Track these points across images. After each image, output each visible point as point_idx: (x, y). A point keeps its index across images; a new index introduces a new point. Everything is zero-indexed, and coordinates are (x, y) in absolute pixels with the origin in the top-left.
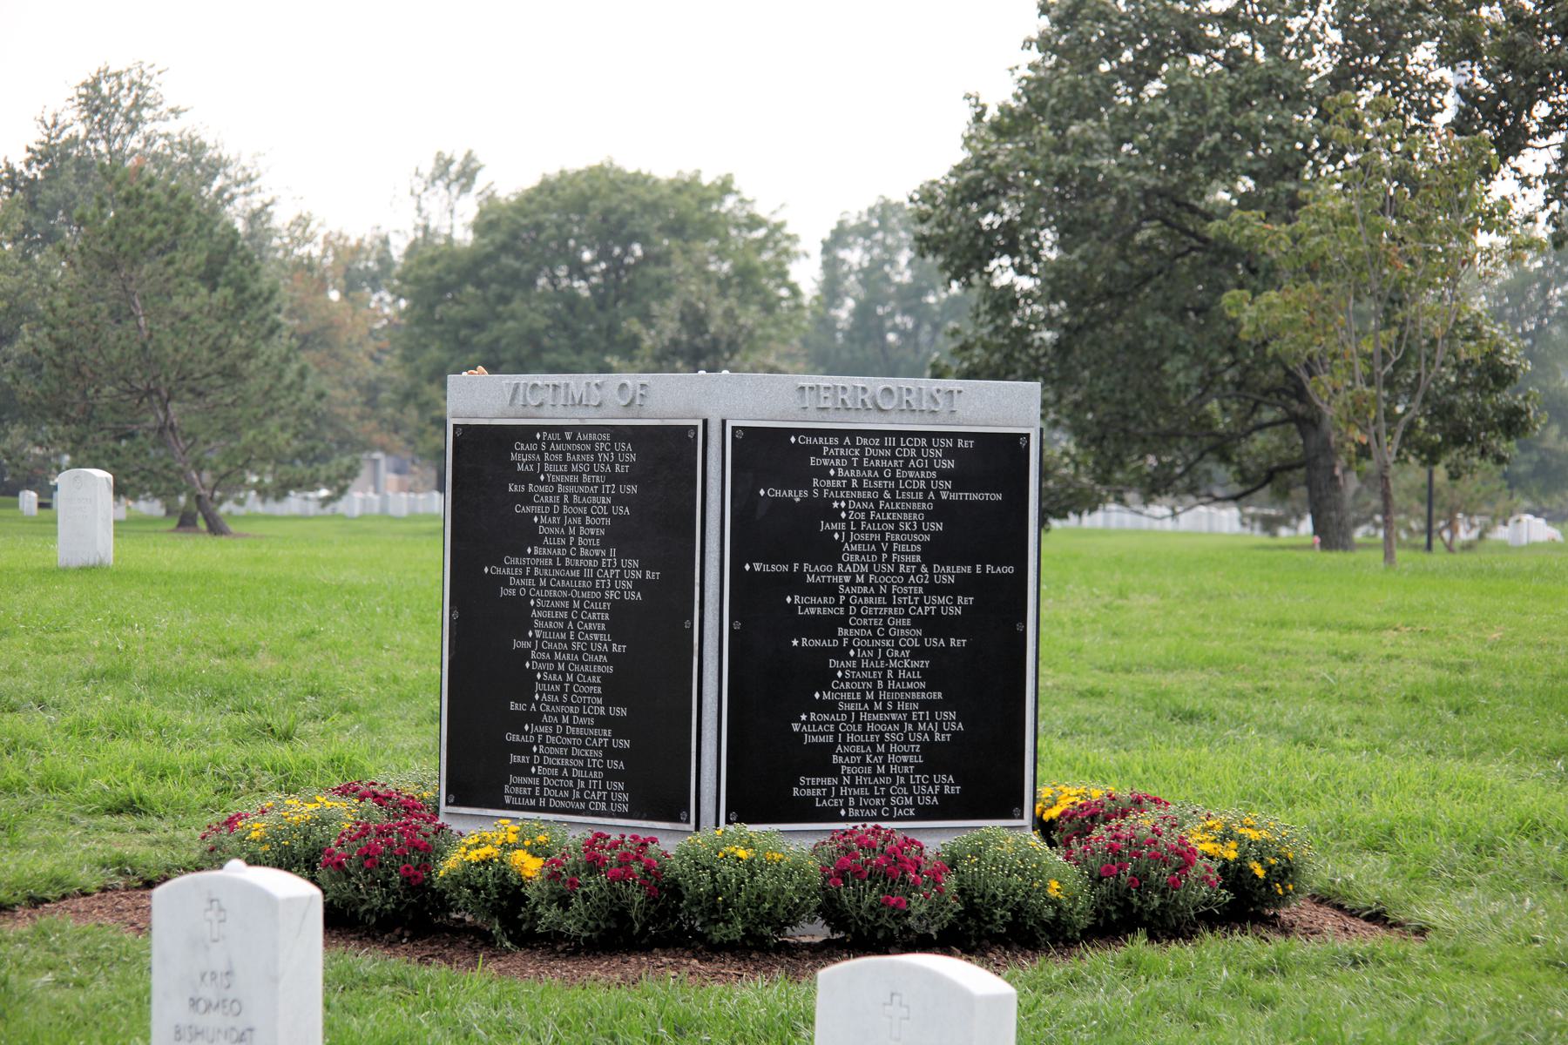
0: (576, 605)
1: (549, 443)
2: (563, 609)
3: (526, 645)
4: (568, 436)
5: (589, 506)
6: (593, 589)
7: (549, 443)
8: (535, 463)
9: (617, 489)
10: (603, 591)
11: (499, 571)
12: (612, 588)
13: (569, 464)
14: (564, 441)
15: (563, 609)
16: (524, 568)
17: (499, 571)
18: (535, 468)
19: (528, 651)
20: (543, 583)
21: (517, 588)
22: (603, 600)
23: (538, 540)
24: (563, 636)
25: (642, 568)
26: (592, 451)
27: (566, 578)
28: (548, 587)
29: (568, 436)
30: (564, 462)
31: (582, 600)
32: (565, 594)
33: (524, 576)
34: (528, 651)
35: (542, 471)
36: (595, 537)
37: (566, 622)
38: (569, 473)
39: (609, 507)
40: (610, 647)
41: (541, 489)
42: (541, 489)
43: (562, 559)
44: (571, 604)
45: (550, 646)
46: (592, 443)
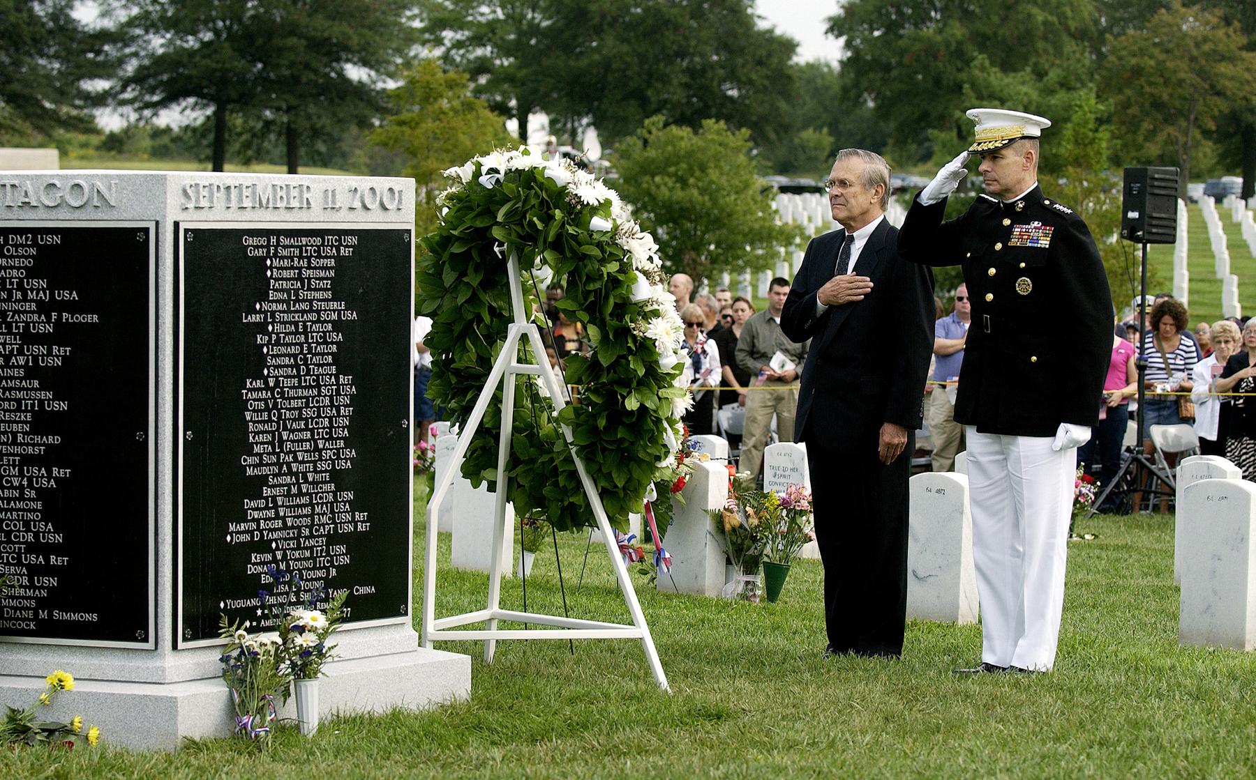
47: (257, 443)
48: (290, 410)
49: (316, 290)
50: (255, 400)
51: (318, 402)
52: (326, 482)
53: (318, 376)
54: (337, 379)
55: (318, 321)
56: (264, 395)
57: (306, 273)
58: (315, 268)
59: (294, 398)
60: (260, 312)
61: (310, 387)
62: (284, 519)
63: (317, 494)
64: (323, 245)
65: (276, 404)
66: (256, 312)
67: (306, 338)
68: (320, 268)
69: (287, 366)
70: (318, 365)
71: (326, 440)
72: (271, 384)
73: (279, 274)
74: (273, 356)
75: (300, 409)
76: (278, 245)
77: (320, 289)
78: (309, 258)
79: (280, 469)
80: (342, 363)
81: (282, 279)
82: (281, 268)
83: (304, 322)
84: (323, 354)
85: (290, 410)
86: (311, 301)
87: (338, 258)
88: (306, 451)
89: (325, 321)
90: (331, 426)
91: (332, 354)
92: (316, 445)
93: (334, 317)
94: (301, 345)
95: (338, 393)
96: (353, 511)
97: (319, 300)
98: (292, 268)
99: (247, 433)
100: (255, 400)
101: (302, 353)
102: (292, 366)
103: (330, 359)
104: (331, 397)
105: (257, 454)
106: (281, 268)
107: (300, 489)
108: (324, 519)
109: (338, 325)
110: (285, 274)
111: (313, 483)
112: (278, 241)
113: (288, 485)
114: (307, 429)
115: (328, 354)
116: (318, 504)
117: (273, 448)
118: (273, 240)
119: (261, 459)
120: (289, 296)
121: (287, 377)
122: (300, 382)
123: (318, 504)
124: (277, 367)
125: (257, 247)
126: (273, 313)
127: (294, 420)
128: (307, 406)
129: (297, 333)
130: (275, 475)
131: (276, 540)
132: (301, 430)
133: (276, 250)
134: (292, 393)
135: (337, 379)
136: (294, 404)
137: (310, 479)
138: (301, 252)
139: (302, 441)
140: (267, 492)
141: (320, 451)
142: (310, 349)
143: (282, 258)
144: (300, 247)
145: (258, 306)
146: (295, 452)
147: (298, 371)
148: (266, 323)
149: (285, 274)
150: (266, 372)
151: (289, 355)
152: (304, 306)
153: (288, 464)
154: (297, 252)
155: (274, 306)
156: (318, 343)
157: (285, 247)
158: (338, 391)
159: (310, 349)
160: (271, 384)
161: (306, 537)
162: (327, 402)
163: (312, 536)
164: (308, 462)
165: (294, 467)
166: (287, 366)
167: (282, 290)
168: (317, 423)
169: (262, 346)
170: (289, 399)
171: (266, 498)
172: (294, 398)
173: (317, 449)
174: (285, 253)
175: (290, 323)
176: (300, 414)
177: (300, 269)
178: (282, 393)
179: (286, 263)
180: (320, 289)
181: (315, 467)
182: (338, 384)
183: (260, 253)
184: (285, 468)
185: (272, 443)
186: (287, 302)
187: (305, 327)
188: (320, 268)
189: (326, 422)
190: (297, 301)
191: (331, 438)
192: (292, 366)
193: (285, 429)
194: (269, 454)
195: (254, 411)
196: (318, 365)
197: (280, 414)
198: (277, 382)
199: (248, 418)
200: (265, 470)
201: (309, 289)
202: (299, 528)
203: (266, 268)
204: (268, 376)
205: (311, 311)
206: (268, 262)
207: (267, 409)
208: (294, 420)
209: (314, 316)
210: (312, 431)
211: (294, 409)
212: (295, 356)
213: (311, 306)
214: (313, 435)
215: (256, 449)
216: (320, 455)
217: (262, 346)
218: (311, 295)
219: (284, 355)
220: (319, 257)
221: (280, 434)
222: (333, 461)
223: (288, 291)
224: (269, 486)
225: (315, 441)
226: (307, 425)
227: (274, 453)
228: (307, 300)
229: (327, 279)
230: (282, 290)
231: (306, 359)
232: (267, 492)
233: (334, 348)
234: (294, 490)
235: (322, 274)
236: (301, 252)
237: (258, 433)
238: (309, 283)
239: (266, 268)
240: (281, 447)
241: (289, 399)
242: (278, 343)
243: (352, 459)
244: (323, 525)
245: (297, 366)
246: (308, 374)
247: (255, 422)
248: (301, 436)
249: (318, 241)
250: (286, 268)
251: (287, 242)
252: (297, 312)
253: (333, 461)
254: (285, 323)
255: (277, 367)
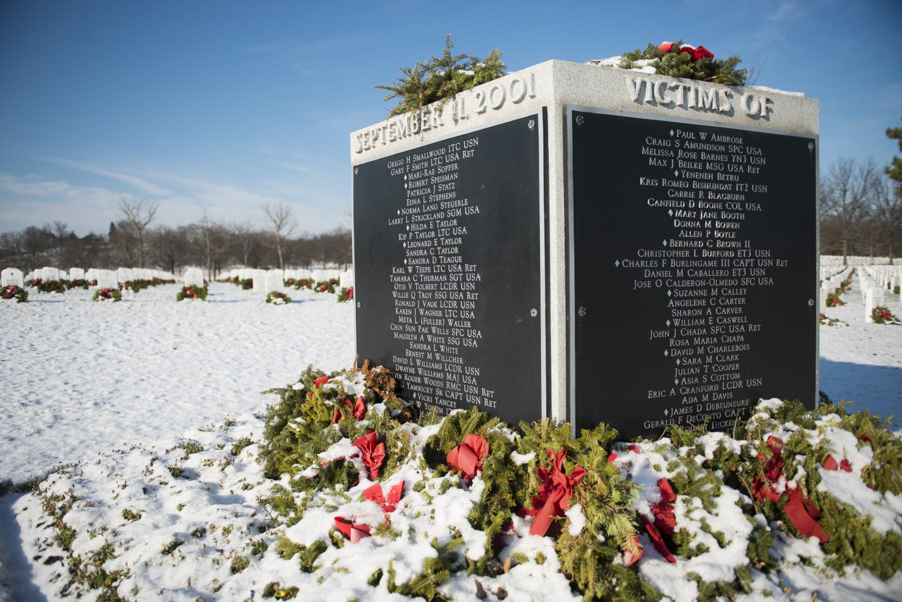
0: (714, 292)
1: (683, 141)
2: (700, 298)
3: (661, 334)
4: (703, 136)
5: (724, 202)
6: (730, 277)
7: (683, 141)
8: (669, 159)
9: (750, 188)
10: (739, 278)
11: (632, 264)
12: (748, 275)
13: (704, 163)
14: (698, 140)
15: (700, 298)
16: (659, 260)
17: (632, 264)
18: (669, 163)
19: (667, 340)
20: (680, 274)
21: (653, 279)
22: (739, 286)
23: (674, 234)
24: (703, 322)
25: (773, 257)
26: (726, 153)
27: (704, 269)
28: (686, 277)
29: (703, 136)
30: (699, 160)
31: (720, 288)
32: (702, 283)
33: (660, 268)
34: (667, 340)
35: (676, 167)
36: (730, 230)
37: (704, 309)
38: (704, 170)
39: (743, 204)
40: (746, 327)
41: (674, 184)
42: (674, 184)
43: (699, 251)
44: (709, 292)
45: (689, 333)
46: (726, 145)
47: (401, 315)
48: (425, 291)
49: (442, 192)
50: (399, 283)
51: (447, 286)
52: (455, 355)
53: (446, 265)
54: (463, 268)
55: (446, 218)
56: (404, 279)
57: (434, 180)
58: (441, 174)
59: (428, 283)
60: (400, 216)
61: (440, 274)
62: (422, 377)
63: (448, 363)
64: (447, 153)
65: (414, 286)
66: (398, 217)
67: (436, 234)
68: (445, 174)
69: (421, 257)
70: (447, 256)
71: (455, 319)
72: (410, 271)
73: (413, 185)
74: (411, 249)
75: (433, 292)
76: (412, 162)
77: (447, 191)
78: (436, 167)
79: (419, 337)
80: (467, 253)
81: (416, 188)
82: (416, 180)
83: (434, 220)
84: (450, 246)
85: (425, 291)
86: (439, 203)
87: (460, 162)
88: (438, 327)
89: (451, 218)
90: (459, 309)
91: (458, 245)
92: (447, 323)
93: (459, 213)
94: (432, 239)
95: (464, 280)
96: (480, 385)
97: (445, 201)
98: (423, 178)
99: (394, 307)
100: (399, 283)
101: (433, 245)
102: (426, 257)
103: (456, 250)
104: (458, 283)
105: (401, 324)
106: (416, 180)
107: (434, 356)
108: (454, 386)
109: (462, 221)
110: (418, 184)
111: (445, 354)
112: (412, 159)
113: (425, 352)
114: (438, 309)
115: (454, 246)
116: (449, 372)
117: (413, 321)
118: (408, 159)
119: (404, 328)
120: (422, 201)
121: (422, 265)
122: (432, 270)
123: (449, 372)
124: (415, 257)
125: (397, 168)
126: (410, 216)
127: (429, 300)
128: (438, 290)
129: (428, 230)
130: (415, 342)
131: (416, 392)
132: (434, 309)
133: (411, 167)
134: (426, 278)
135: (463, 268)
136: (427, 287)
137: (443, 350)
138: (429, 164)
139: (435, 318)
140: (408, 353)
141: (450, 328)
142: (439, 242)
143: (416, 172)
144: (429, 160)
145: (399, 212)
146: (430, 326)
147: (431, 261)
148: (405, 225)
149: (418, 184)
150: (405, 262)
151: (423, 249)
152: (433, 208)
153: (425, 335)
154: (426, 164)
155: (410, 211)
156: (446, 237)
157: (417, 163)
158: (464, 277)
159: (439, 242)
160: (410, 271)
161: (440, 397)
162: (455, 286)
163: (444, 398)
164: (440, 336)
165: (429, 337)
166: (421, 257)
167: (417, 197)
168: (447, 304)
169: (402, 242)
170: (425, 283)
171: (408, 358)
172: (428, 283)
173: (447, 326)
174: (417, 167)
175: (423, 222)
176: (433, 296)
177: (429, 177)
178: (419, 278)
179: (418, 175)
180: (447, 191)
181: (446, 341)
182: (464, 272)
183: (399, 172)
184: (422, 337)
185: (412, 316)
186: (420, 206)
187: (435, 224)
188: (445, 174)
189: (455, 304)
190: (428, 204)
191: (459, 319)
192: (426, 257)
193: (422, 306)
194: (410, 324)
195: (398, 291)
196: (447, 256)
197: (417, 295)
198: (414, 270)
199: (395, 296)
200: (407, 337)
201: (437, 193)
202: (434, 388)
203: (404, 182)
204: (407, 265)
205: (439, 211)
206: (405, 178)
207: (407, 290)
208: (429, 300)
209: (441, 215)
210: (443, 310)
211: (428, 291)
212: (428, 249)
213: (439, 206)
214: (443, 314)
215: (401, 320)
216: (450, 332)
217: (402, 242)
218: (439, 197)
219: (419, 248)
220: (445, 164)
221: (418, 312)
222: (461, 338)
223: (420, 197)
224: (410, 350)
225: (446, 319)
226: (438, 304)
227: (413, 324)
228: (436, 202)
229: (451, 181)
230: (417, 197)
231: (436, 251)
232: (408, 353)
233: (460, 241)
234: (430, 356)
235: (447, 178)
236: (429, 164)
237: (402, 307)
238: (437, 188)
239: (404, 182)
240: (418, 320)
241: (425, 283)
242: (414, 239)
243: (478, 340)
244: (454, 391)
245: (430, 257)
246: (438, 262)
247: (399, 299)
248: (434, 313)
249: (443, 151)
250: (418, 180)
251: (418, 158)
252: (428, 212)
253: (461, 338)
254: (419, 223)
255: (415, 257)
